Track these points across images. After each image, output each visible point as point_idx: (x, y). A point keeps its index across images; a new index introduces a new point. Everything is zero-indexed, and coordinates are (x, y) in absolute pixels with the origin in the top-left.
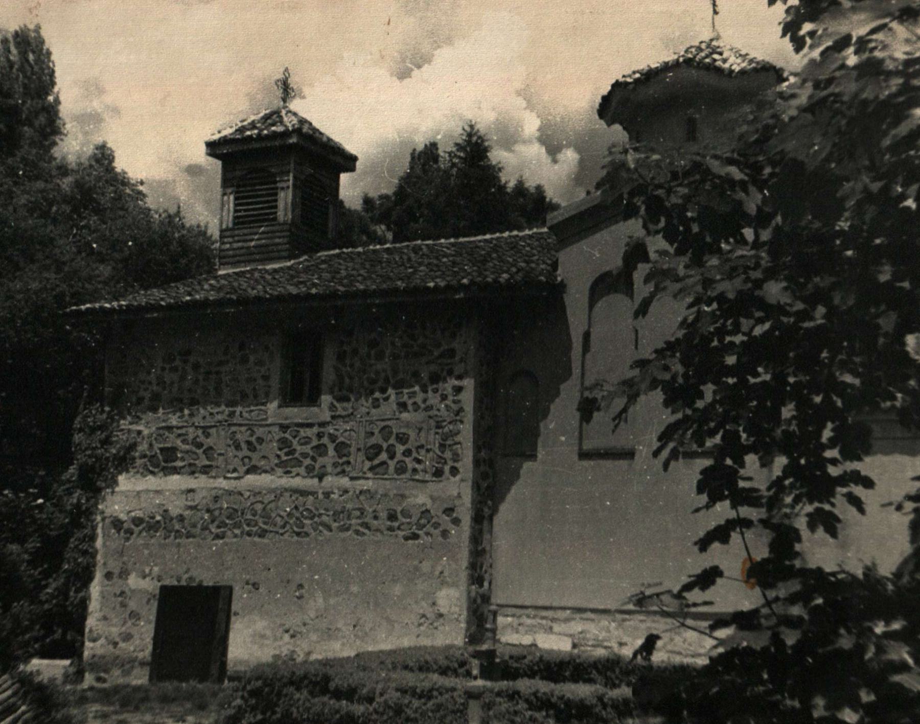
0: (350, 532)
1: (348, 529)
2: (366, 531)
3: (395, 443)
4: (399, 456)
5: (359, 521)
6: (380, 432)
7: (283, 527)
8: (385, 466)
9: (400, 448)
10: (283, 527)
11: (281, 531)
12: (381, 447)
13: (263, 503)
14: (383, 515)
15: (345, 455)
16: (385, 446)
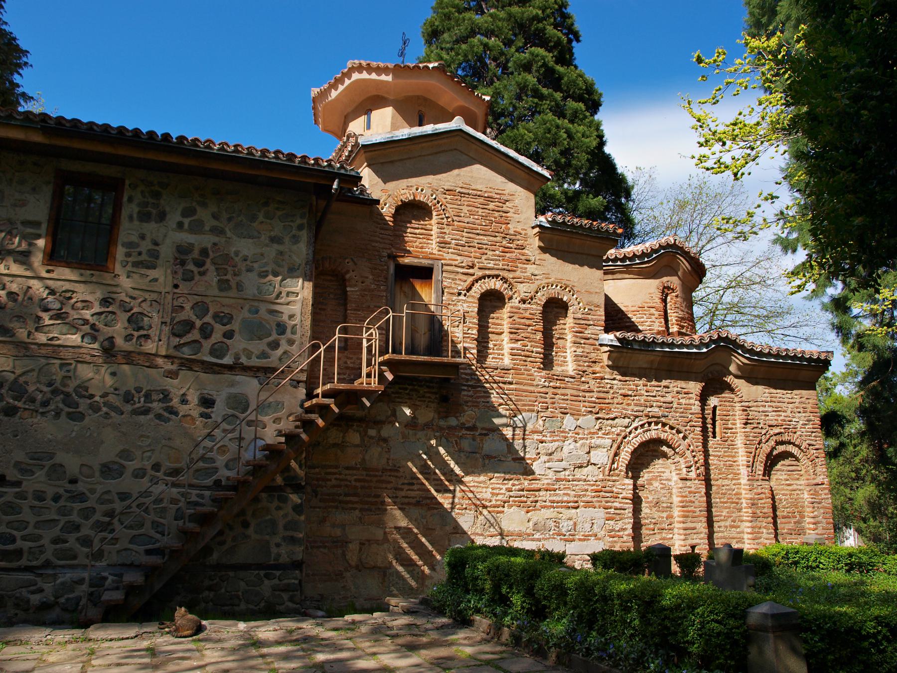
0: (149, 417)
1: (146, 412)
2: (173, 417)
3: (212, 322)
4: (217, 337)
5: (161, 405)
6: (192, 308)
7: (45, 404)
8: (197, 345)
9: (219, 330)
10: (45, 404)
11: (41, 410)
12: (194, 323)
13: (13, 372)
14: (196, 401)
15: (140, 328)
16: (198, 323)
